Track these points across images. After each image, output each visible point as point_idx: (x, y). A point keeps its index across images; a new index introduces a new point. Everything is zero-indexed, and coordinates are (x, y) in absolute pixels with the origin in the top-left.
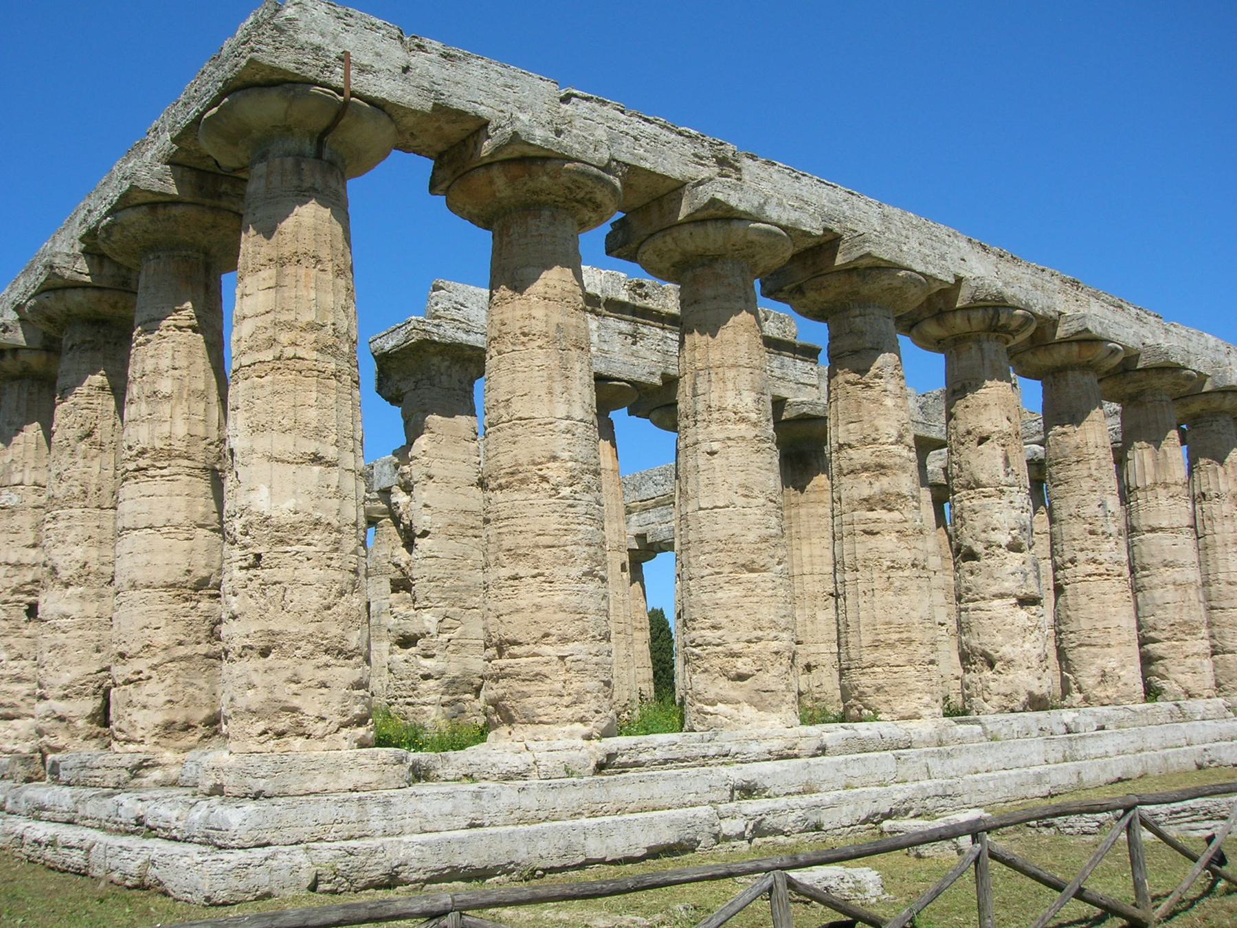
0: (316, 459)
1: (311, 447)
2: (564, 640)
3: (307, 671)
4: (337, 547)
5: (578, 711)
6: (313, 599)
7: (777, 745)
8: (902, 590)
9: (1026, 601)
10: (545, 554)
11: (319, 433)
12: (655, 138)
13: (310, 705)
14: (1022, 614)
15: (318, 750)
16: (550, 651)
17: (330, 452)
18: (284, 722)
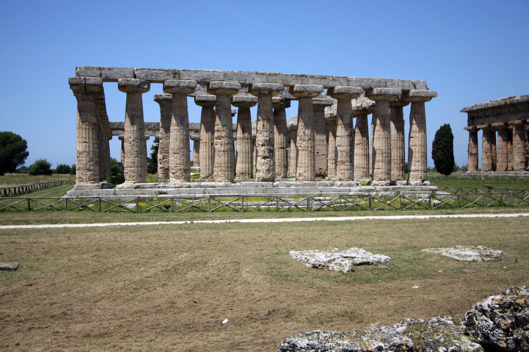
0: (85, 142)
1: (84, 140)
2: (131, 167)
3: (83, 173)
4: (89, 155)
5: (133, 179)
6: (84, 162)
7: (177, 186)
8: (221, 156)
9: (265, 158)
10: (129, 154)
11: (85, 138)
12: (157, 73)
13: (84, 178)
14: (263, 160)
15: (85, 184)
16: (129, 169)
17: (87, 141)
18: (81, 180)
